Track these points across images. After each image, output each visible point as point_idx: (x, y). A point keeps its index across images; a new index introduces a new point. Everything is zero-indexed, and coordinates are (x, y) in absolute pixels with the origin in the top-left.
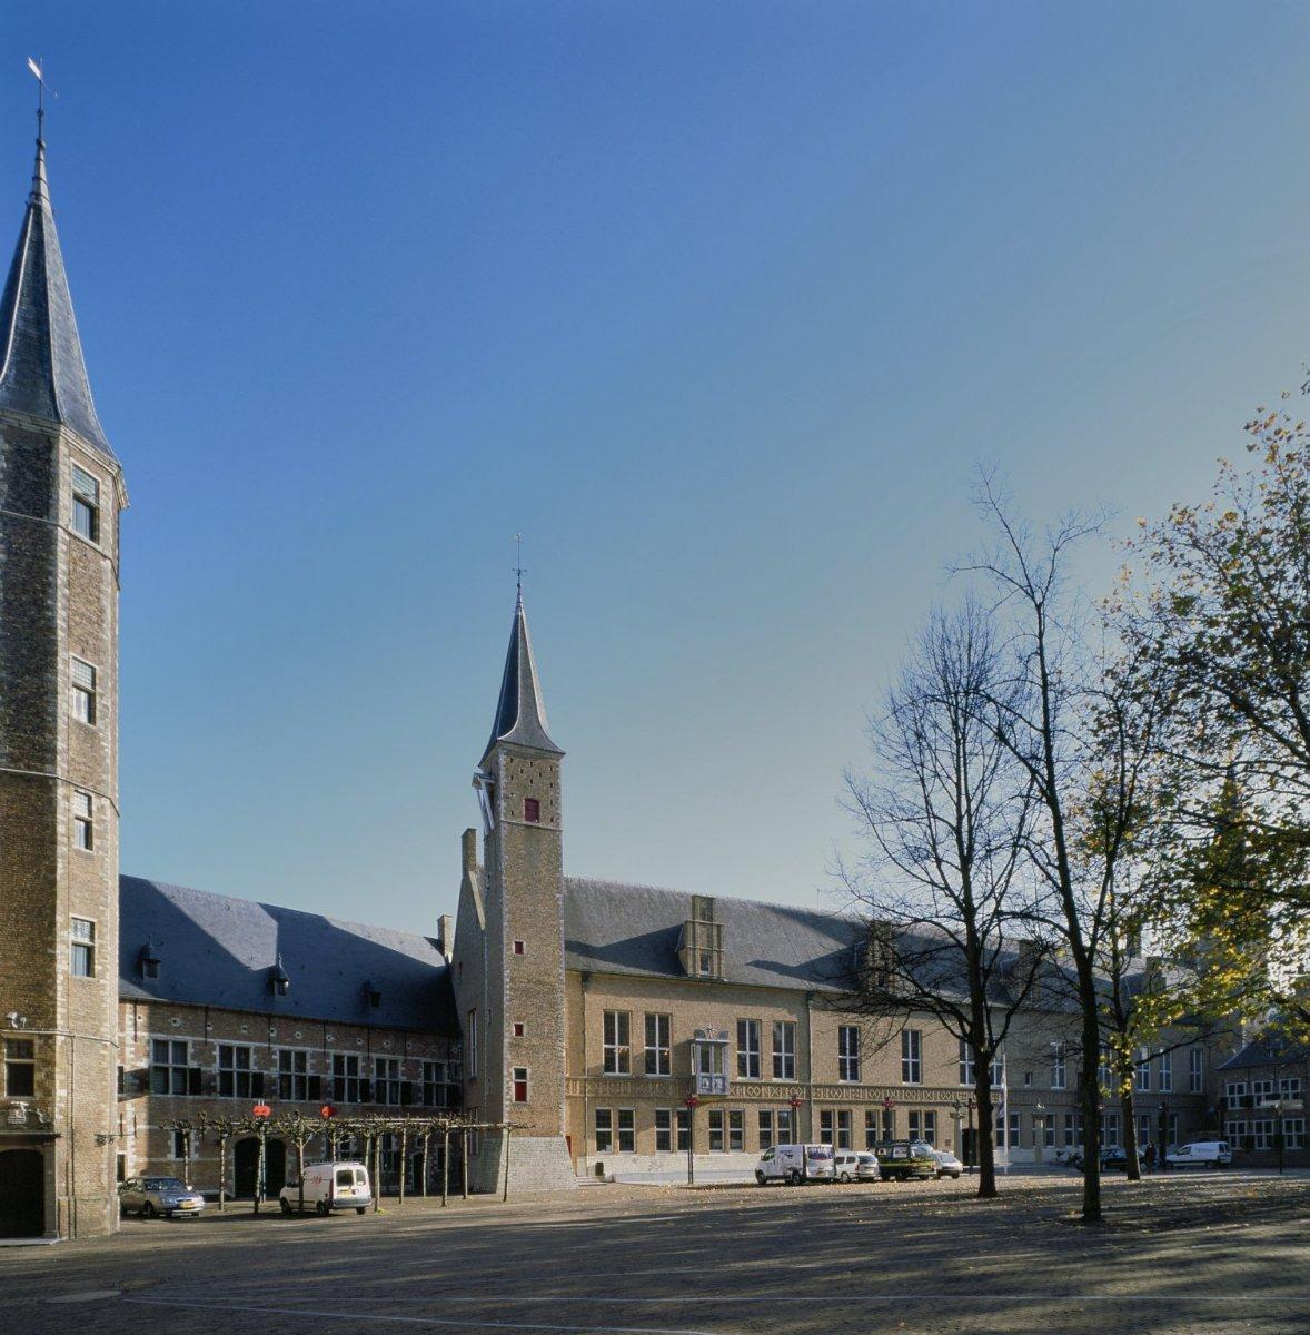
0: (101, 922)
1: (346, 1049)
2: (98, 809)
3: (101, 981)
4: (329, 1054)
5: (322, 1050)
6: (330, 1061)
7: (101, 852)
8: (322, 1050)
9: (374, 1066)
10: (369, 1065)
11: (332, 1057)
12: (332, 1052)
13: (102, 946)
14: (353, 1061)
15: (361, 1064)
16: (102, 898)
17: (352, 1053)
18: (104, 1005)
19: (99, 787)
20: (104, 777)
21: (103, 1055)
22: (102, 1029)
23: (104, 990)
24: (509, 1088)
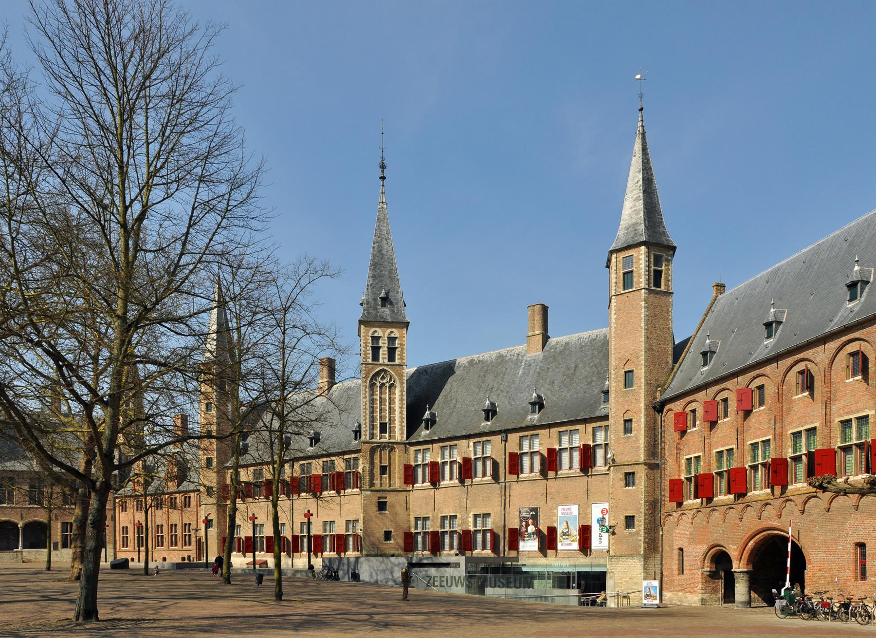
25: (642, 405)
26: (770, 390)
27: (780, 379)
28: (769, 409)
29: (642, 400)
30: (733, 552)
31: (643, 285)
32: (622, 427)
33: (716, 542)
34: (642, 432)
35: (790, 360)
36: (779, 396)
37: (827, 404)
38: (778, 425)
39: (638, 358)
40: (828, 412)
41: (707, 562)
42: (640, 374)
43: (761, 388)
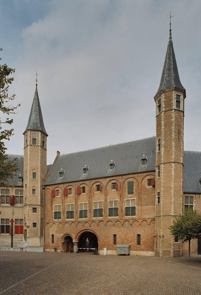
3: (161, 203)
13: (161, 196)
22: (161, 214)
25: (39, 185)
26: (87, 189)
27: (91, 186)
28: (87, 194)
29: (39, 183)
30: (73, 236)
31: (40, 145)
32: (31, 192)
33: (67, 233)
34: (39, 194)
35: (94, 181)
36: (90, 191)
37: (106, 196)
38: (90, 199)
39: (38, 169)
40: (106, 198)
41: (63, 239)
42: (38, 174)
43: (84, 188)
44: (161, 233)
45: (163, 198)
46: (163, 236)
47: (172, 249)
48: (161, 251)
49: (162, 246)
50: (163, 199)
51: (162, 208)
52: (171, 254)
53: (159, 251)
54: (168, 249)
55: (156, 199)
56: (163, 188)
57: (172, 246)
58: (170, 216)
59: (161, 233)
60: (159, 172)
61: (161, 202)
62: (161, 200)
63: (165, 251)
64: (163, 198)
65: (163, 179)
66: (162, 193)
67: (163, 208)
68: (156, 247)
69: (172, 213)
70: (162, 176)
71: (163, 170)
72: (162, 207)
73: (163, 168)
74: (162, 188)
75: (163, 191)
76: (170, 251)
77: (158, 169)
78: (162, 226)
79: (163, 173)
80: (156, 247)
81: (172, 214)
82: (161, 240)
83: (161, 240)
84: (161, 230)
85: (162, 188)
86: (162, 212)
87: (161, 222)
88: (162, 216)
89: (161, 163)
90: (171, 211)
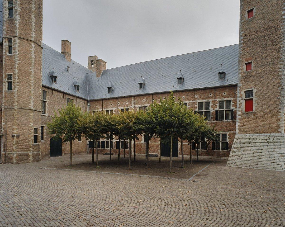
0: (14, 74)
1: (203, 99)
2: (14, 41)
3: (14, 91)
4: (196, 102)
5: (193, 101)
6: (197, 105)
7: (14, 53)
8: (193, 101)
9: (218, 105)
10: (215, 105)
11: (197, 104)
12: (198, 101)
13: (14, 80)
14: (207, 103)
15: (211, 104)
16: (14, 67)
17: (207, 100)
18: (14, 98)
19: (14, 35)
20: (15, 31)
21: (14, 112)
22: (14, 105)
23: (14, 93)
24: (240, 104)
44: (15, 131)
45: (18, 84)
46: (18, 136)
47: (31, 151)
48: (15, 156)
49: (17, 148)
50: (17, 85)
51: (16, 97)
52: (30, 159)
53: (12, 155)
54: (25, 153)
55: (4, 84)
56: (19, 70)
57: (31, 149)
58: (29, 110)
59: (14, 131)
60: (10, 47)
61: (16, 88)
62: (16, 87)
63: (21, 155)
64: (18, 84)
65: (18, 59)
66: (17, 78)
67: (18, 97)
68: (5, 150)
69: (31, 106)
70: (17, 54)
71: (19, 46)
72: (17, 96)
73: (19, 43)
74: (17, 71)
75: (18, 74)
76: (28, 156)
77: (7, 42)
78: (17, 122)
79: (18, 50)
80: (5, 150)
81: (32, 108)
82: (14, 141)
83: (14, 141)
84: (14, 126)
85: (17, 71)
86: (16, 103)
87: (16, 117)
88: (16, 109)
89: (15, 35)
90: (31, 103)
